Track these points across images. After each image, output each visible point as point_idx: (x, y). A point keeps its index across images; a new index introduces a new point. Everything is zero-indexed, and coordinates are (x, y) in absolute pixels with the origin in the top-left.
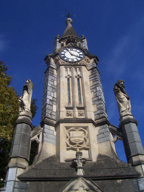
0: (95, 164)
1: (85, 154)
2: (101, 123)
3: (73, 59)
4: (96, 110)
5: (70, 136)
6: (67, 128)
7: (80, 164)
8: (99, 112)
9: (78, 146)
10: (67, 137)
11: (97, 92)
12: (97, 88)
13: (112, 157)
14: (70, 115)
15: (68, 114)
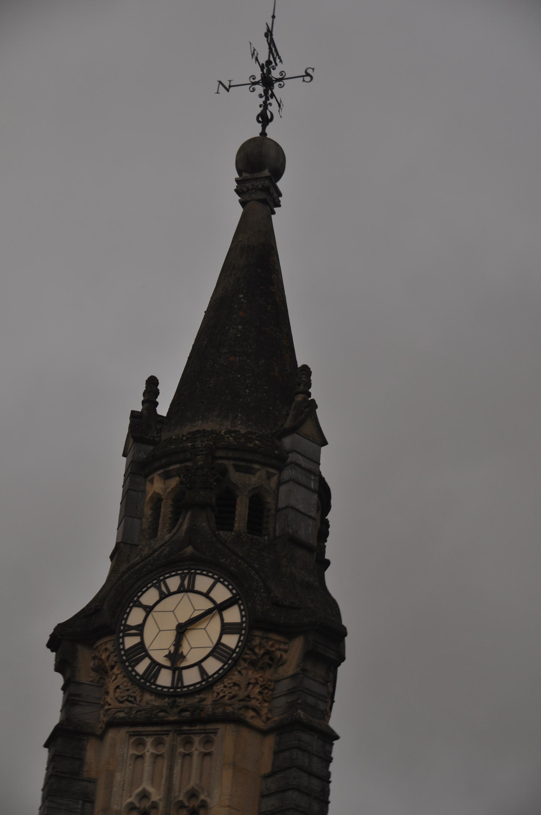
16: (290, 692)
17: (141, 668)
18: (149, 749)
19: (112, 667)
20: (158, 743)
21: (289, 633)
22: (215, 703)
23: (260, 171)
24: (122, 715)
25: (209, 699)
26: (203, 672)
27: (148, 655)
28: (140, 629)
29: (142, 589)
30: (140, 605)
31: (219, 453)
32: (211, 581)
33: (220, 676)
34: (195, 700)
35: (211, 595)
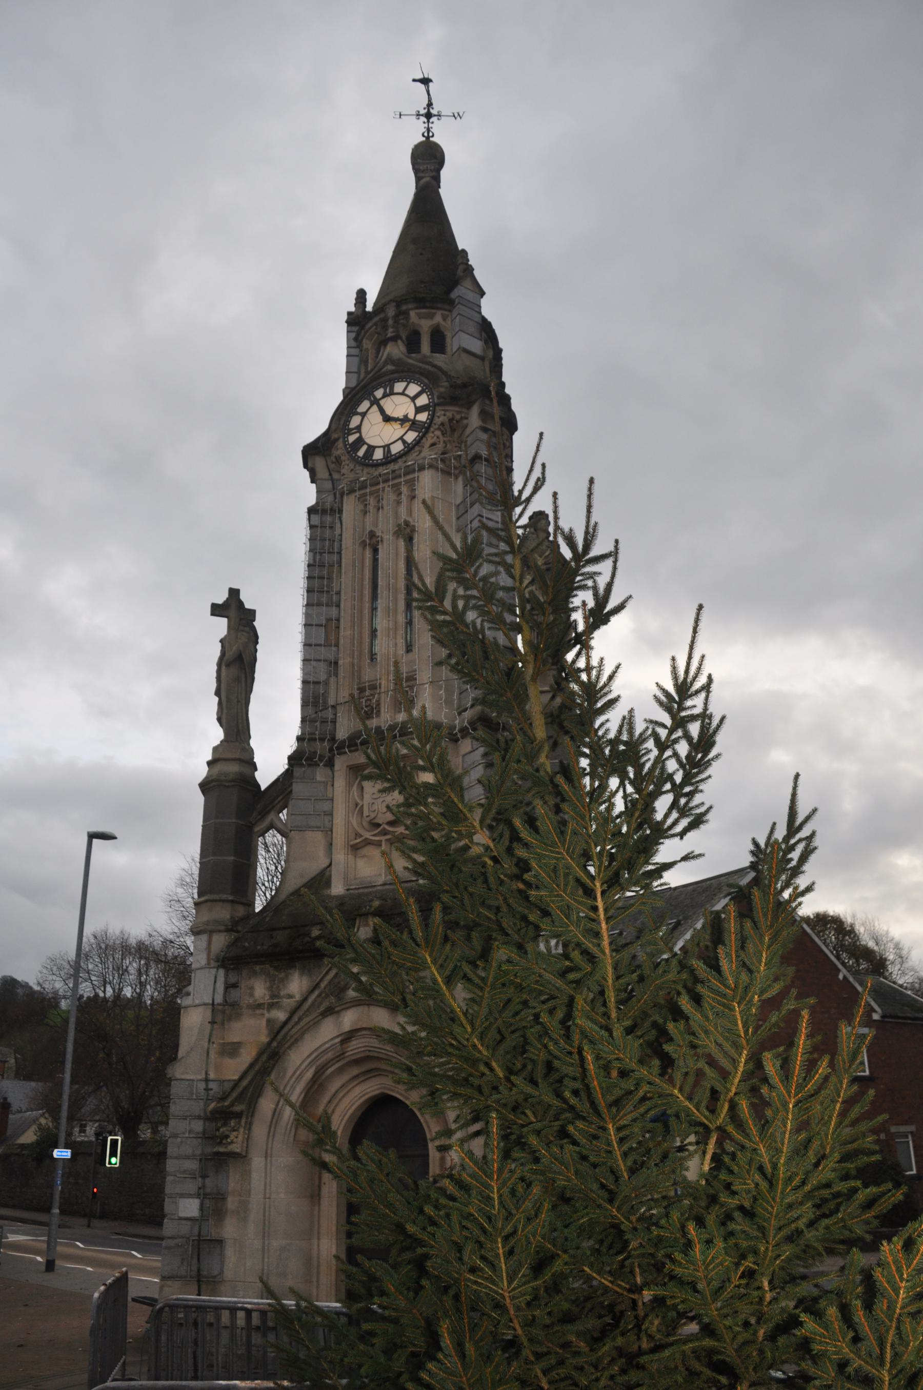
9: (384, 833)
17: (361, 453)
26: (404, 442)
27: (365, 443)
28: (359, 428)
32: (405, 384)
33: (417, 442)
35: (406, 392)
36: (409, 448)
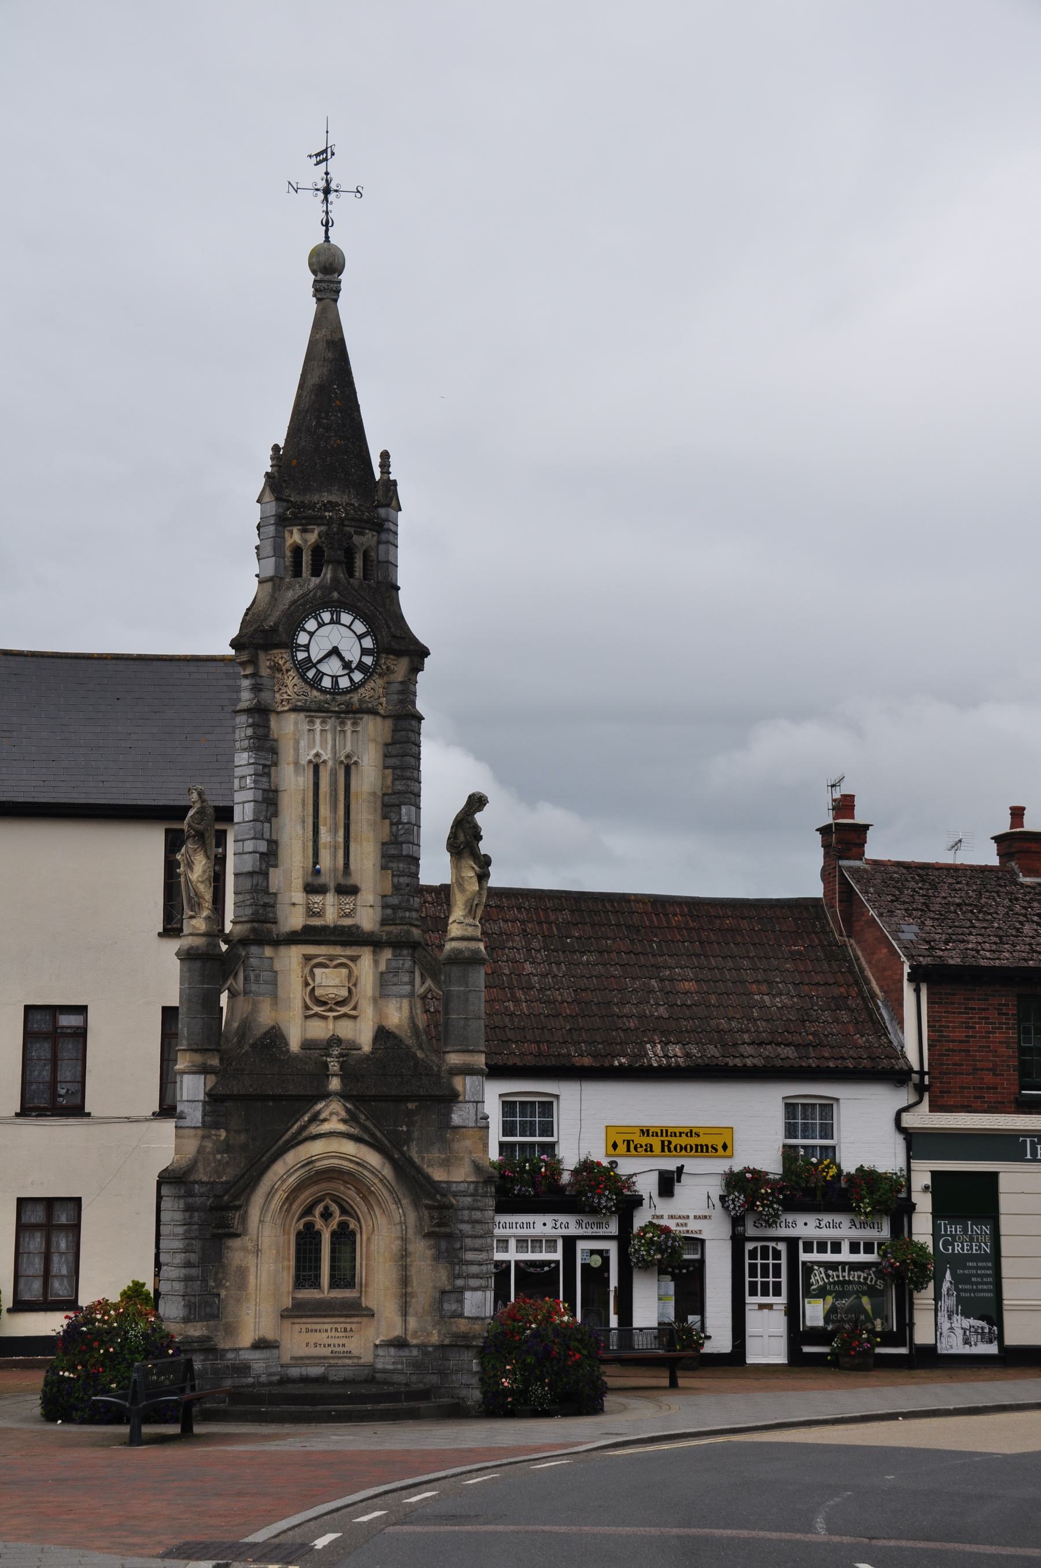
0: (367, 1058)
1: (345, 1030)
2: (396, 945)
3: (337, 677)
4: (389, 891)
5: (314, 981)
6: (307, 958)
7: (334, 1066)
8: (395, 901)
9: (331, 1010)
10: (307, 984)
11: (400, 827)
12: (404, 809)
13: (409, 1042)
14: (319, 914)
15: (311, 913)
16: (400, 693)
17: (311, 674)
18: (318, 726)
19: (288, 671)
20: (323, 722)
21: (399, 654)
22: (360, 701)
23: (327, 269)
24: (300, 704)
25: (355, 698)
28: (307, 648)
29: (305, 619)
30: (305, 630)
31: (346, 523)
33: (362, 683)
34: (348, 697)
36: (355, 687)
